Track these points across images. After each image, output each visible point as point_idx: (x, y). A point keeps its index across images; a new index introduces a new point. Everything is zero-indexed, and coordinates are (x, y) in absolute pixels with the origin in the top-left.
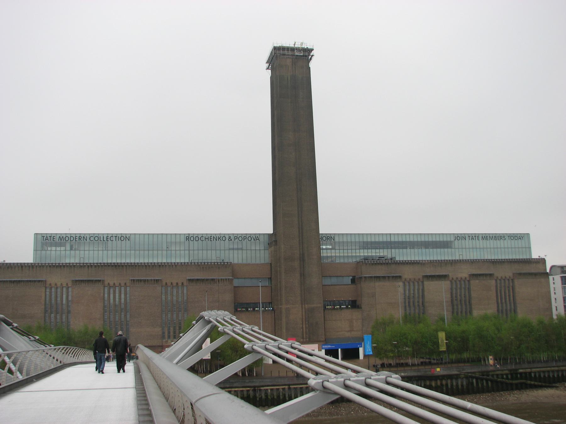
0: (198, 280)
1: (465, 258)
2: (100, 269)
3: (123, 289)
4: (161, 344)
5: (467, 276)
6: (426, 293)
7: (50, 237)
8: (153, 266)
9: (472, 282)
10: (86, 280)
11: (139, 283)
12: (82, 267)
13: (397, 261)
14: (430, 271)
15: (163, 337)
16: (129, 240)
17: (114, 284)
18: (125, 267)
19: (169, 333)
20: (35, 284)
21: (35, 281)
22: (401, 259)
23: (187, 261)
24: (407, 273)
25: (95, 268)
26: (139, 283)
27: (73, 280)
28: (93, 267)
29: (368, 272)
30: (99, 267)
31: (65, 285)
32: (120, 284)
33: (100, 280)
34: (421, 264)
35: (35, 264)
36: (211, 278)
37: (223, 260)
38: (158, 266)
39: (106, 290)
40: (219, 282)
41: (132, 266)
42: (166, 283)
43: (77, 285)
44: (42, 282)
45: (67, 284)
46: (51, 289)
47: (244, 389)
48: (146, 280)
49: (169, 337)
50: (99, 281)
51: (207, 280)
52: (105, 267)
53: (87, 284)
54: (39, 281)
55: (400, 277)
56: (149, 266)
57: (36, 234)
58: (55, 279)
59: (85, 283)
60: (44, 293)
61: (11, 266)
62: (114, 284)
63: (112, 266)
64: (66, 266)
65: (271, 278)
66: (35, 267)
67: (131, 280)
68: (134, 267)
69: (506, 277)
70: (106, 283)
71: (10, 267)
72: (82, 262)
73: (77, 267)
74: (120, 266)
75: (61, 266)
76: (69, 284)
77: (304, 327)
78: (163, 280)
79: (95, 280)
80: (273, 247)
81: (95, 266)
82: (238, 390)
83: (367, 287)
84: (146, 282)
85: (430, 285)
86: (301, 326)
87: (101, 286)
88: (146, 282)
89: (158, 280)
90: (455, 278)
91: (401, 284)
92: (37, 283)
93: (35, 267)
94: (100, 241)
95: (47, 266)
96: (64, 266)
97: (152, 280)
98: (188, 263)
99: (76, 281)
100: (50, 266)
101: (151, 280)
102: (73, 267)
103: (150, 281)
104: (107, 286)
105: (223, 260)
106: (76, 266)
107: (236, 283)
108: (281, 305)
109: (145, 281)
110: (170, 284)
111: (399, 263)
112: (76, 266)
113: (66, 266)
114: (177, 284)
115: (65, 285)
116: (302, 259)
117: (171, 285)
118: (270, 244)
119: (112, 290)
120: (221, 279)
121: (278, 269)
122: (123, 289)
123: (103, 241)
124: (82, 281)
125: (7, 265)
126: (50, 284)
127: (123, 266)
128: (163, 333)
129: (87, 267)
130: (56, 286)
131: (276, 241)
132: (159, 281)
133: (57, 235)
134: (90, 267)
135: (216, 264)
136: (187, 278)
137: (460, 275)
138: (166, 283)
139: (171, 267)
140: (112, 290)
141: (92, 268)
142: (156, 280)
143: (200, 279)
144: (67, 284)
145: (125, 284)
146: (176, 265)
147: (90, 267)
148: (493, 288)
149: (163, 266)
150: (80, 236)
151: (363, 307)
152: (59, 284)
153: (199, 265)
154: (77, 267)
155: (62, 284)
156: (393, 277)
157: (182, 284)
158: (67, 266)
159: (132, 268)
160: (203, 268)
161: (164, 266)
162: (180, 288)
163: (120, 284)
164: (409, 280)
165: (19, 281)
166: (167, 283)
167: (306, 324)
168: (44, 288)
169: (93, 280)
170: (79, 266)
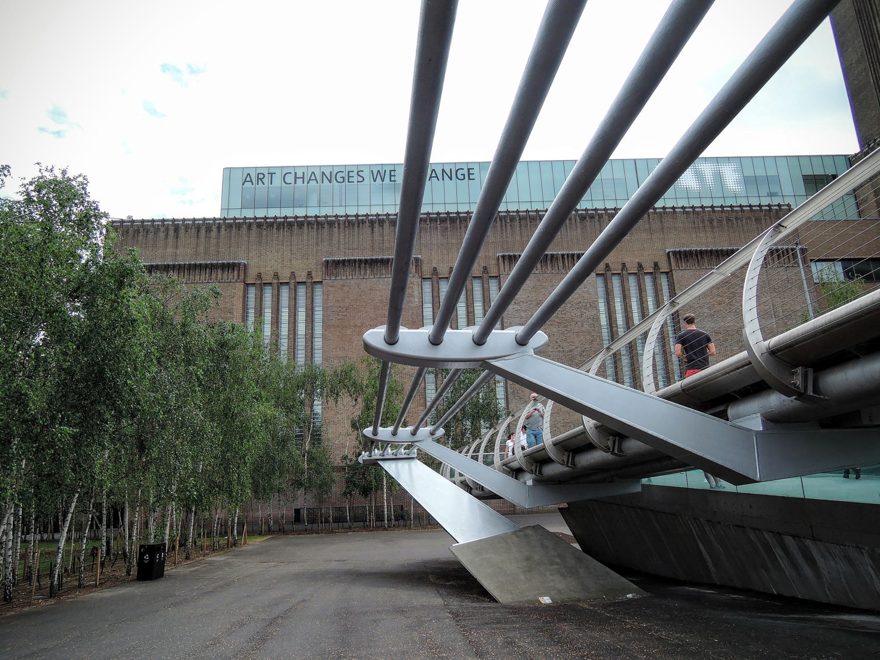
10: (366, 260)
12: (353, 224)
20: (214, 276)
25: (392, 228)
27: (327, 262)
28: (387, 224)
38: (578, 220)
41: (501, 220)
44: (233, 270)
45: (309, 274)
53: (368, 272)
60: (241, 300)
61: (143, 226)
63: (443, 220)
64: (306, 224)
66: (214, 229)
67: (503, 257)
68: (508, 221)
70: (426, 269)
71: (141, 230)
73: (339, 224)
76: (313, 274)
84: (549, 262)
88: (549, 262)
92: (220, 272)
93: (214, 229)
96: (301, 225)
97: (566, 256)
99: (337, 263)
101: (563, 255)
113: (306, 224)
117: (622, 269)
125: (132, 226)
126: (259, 276)
130: (275, 281)
134: (377, 225)
141: (383, 226)
143: (706, 251)
144: (309, 274)
145: (485, 268)
147: (377, 225)
149: (592, 217)
153: (698, 213)
154: (339, 224)
155: (293, 274)
157: (656, 265)
158: (309, 223)
159: (502, 226)
160: (711, 221)
161: (597, 217)
162: (648, 280)
168: (242, 285)
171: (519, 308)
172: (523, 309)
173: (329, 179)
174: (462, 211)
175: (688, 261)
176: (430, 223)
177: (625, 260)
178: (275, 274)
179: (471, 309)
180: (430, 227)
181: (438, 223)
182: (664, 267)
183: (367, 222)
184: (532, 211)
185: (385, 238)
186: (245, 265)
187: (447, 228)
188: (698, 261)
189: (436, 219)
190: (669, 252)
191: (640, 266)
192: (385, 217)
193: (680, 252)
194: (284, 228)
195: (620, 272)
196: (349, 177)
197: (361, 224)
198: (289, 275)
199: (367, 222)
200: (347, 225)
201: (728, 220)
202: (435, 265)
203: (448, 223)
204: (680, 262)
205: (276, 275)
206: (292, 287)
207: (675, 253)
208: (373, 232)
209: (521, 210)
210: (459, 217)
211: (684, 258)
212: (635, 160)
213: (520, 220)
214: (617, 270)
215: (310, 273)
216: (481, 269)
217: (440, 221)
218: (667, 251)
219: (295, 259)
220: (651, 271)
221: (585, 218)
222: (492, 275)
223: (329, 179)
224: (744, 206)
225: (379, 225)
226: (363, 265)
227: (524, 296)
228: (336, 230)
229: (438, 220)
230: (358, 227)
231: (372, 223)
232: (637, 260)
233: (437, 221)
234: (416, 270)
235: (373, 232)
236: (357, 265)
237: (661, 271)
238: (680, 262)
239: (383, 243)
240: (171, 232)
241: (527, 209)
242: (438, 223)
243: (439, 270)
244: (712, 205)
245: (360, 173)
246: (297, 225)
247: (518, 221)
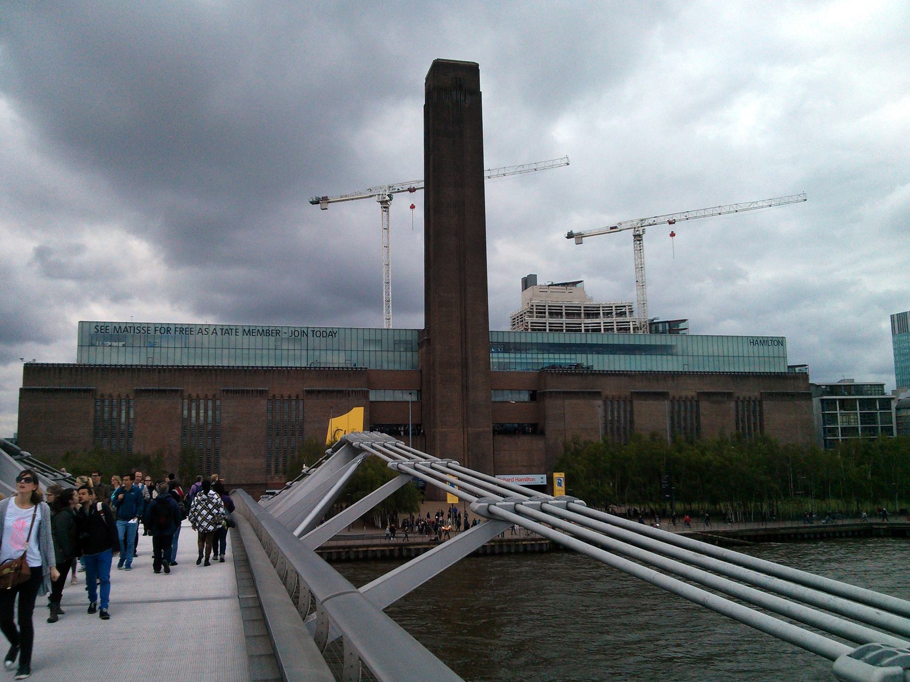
0: (319, 392)
1: (691, 370)
2: (177, 374)
3: (210, 404)
4: (265, 482)
5: (694, 394)
6: (635, 418)
7: (130, 327)
9: (701, 404)
13: (595, 371)
14: (641, 387)
15: (268, 471)
17: (198, 395)
18: (213, 372)
19: (277, 465)
21: (79, 391)
22: (601, 368)
23: (304, 364)
24: (610, 388)
27: (137, 390)
29: (554, 385)
31: (123, 396)
33: (178, 390)
34: (629, 376)
35: (79, 365)
37: (355, 365)
40: (348, 395)
42: (274, 395)
46: (103, 401)
47: (385, 548)
48: (244, 390)
49: (277, 472)
50: (177, 391)
54: (85, 391)
55: (599, 393)
57: (81, 323)
58: (107, 387)
62: (198, 395)
63: (196, 370)
65: (421, 390)
67: (224, 390)
69: (750, 398)
70: (186, 394)
72: (150, 363)
73: (143, 370)
77: (466, 459)
80: (424, 348)
81: (170, 370)
82: (377, 550)
83: (552, 406)
85: (642, 407)
86: (462, 458)
89: (263, 390)
90: (677, 397)
91: (600, 402)
92: (83, 394)
98: (305, 367)
100: (103, 369)
101: (252, 390)
105: (355, 365)
107: (373, 396)
108: (434, 427)
109: (243, 391)
111: (598, 374)
112: (141, 371)
114: (290, 396)
115: (123, 396)
116: (465, 365)
118: (420, 345)
119: (194, 404)
120: (352, 391)
121: (432, 379)
122: (210, 404)
126: (102, 396)
127: (211, 370)
128: (269, 466)
131: (429, 340)
133: (197, 326)
135: (351, 369)
136: (304, 389)
137: (684, 394)
138: (274, 395)
140: (194, 404)
142: (260, 390)
144: (127, 396)
148: (733, 413)
150: (182, 328)
151: (547, 433)
152: (115, 394)
155: (119, 395)
156: (589, 392)
160: (327, 375)
164: (611, 397)
165: (56, 390)
167: (468, 455)
169: (166, 390)
182: (301, 397)
196: (148, 330)
232: (289, 393)
240: (57, 371)
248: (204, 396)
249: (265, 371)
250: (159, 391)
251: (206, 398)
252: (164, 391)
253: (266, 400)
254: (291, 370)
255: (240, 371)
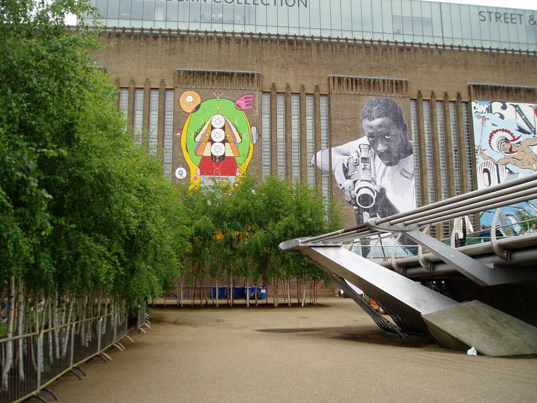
0: (495, 89)
8: (385, 49)
10: (214, 73)
11: (354, 86)
16: (306, 6)
17: (288, 87)
18: (314, 47)
25: (237, 45)
26: (354, 86)
30: (247, 43)
32: (303, 87)
33: (253, 75)
36: (526, 87)
39: (266, 100)
41: (332, 46)
42: (419, 92)
43: (188, 83)
45: (162, 81)
51: (518, 90)
52: (262, 43)
56: (375, 48)
59: (213, 81)
62: (288, 87)
63: (282, 42)
68: (339, 47)
73: (190, 39)
74: (302, 44)
75: (146, 36)
76: (167, 82)
78: (411, 85)
79: (238, 74)
81: (238, 41)
87: (253, 89)
89: (401, 82)
94: (238, 3)
95: (110, 33)
96: (156, 37)
97: (386, 82)
101: (384, 81)
102: (178, 38)
103: (381, 83)
104: (268, 91)
106: (188, 38)
110: (430, 94)
117: (431, 97)
123: (246, 3)
124: (202, 74)
127: (308, 44)
129: (215, 40)
132: (404, 84)
134: (223, 41)
138: (419, 92)
139: (429, 53)
141: (229, 43)
143: (500, 87)
144: (162, 81)
145: (317, 87)
146: (440, 52)
147: (223, 41)
149: (409, 49)
155: (148, 80)
157: (459, 95)
158: (164, 36)
159: (333, 51)
163: (303, 87)
166: (423, 93)
170: (195, 37)
171: (345, 123)
172: (349, 124)
173: (305, 4)
174: (273, 33)
175: (484, 94)
176: (271, 44)
177: (434, 89)
178: (132, 80)
179: (303, 122)
180: (271, 47)
181: (278, 43)
182: (465, 98)
183: (215, 38)
184: (343, 39)
185: (231, 54)
186: (406, 82)
187: (285, 49)
188: (492, 94)
189: (277, 40)
190: (470, 85)
191: (446, 95)
192: (230, 35)
193: (478, 86)
194: (140, 39)
195: (429, 99)
197: (209, 41)
198: (144, 82)
199: (215, 38)
200: (197, 39)
201: (517, 63)
202: (273, 81)
203: (287, 44)
204: (478, 94)
205: (133, 81)
206: (148, 93)
207: (475, 87)
208: (220, 47)
209: (415, 42)
210: (296, 40)
211: (482, 91)
212: (440, 3)
213: (349, 46)
214: (427, 97)
215: (163, 81)
216: (314, 87)
217: (280, 42)
218: (469, 83)
219: (149, 67)
220: (454, 100)
221: (403, 50)
222: (323, 93)
223: (305, 4)
224: (530, 52)
225: (226, 42)
226: (211, 77)
227: (349, 114)
228: (187, 44)
229: (278, 42)
230: (207, 42)
231: (219, 39)
232: (444, 90)
233: (276, 42)
234: (257, 84)
235: (220, 47)
236: (206, 77)
237: (463, 100)
238: (478, 94)
239: (228, 58)
241: (338, 37)
242: (278, 43)
243: (277, 85)
244: (490, 47)
245: (482, 13)
246: (153, 37)
247: (347, 48)
248: (299, 87)
249: (401, 49)
250: (221, 74)
251: (301, 94)
252: (230, 75)
253: (408, 99)
254: (444, 49)
255: (359, 47)
